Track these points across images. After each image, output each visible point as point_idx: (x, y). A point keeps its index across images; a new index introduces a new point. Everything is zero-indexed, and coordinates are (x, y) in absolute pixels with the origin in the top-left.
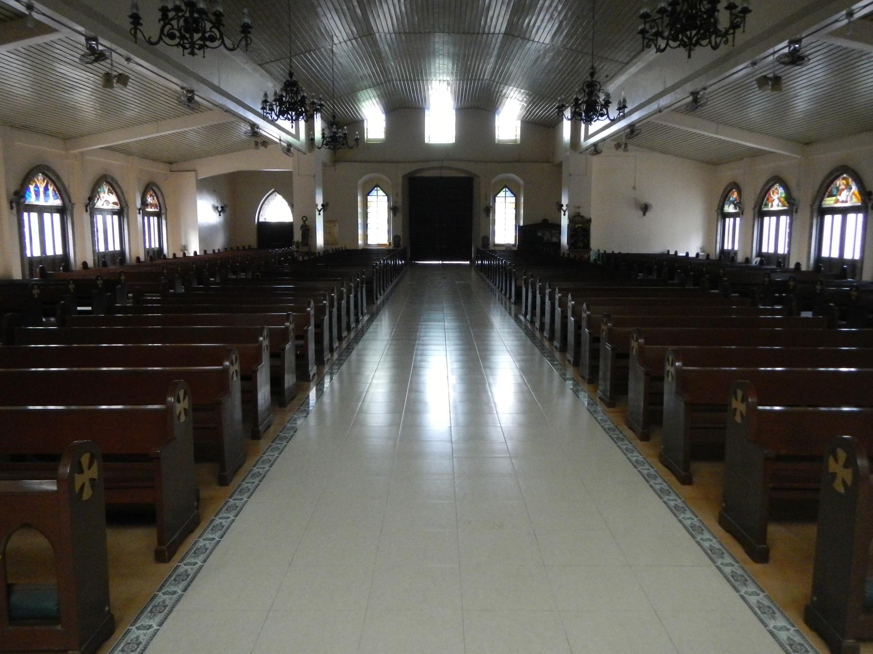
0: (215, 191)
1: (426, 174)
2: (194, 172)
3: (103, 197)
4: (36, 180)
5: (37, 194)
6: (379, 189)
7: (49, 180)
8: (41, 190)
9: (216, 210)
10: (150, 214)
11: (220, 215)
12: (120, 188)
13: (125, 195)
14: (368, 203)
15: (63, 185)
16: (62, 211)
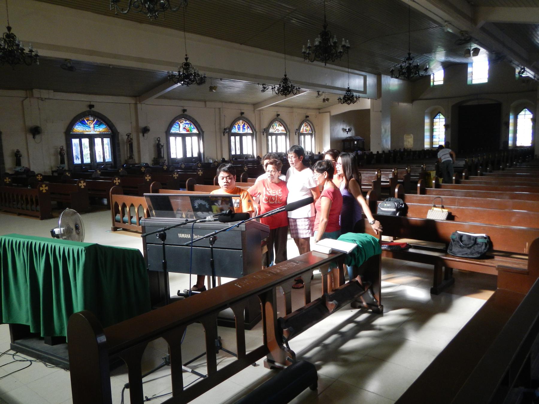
0: (344, 121)
1: (470, 103)
2: (328, 114)
3: (276, 128)
4: (238, 123)
5: (239, 129)
6: (440, 114)
7: (245, 123)
8: (241, 127)
9: (345, 131)
10: (304, 135)
11: (347, 134)
12: (285, 123)
13: (289, 127)
14: (434, 123)
15: (252, 124)
16: (252, 135)
